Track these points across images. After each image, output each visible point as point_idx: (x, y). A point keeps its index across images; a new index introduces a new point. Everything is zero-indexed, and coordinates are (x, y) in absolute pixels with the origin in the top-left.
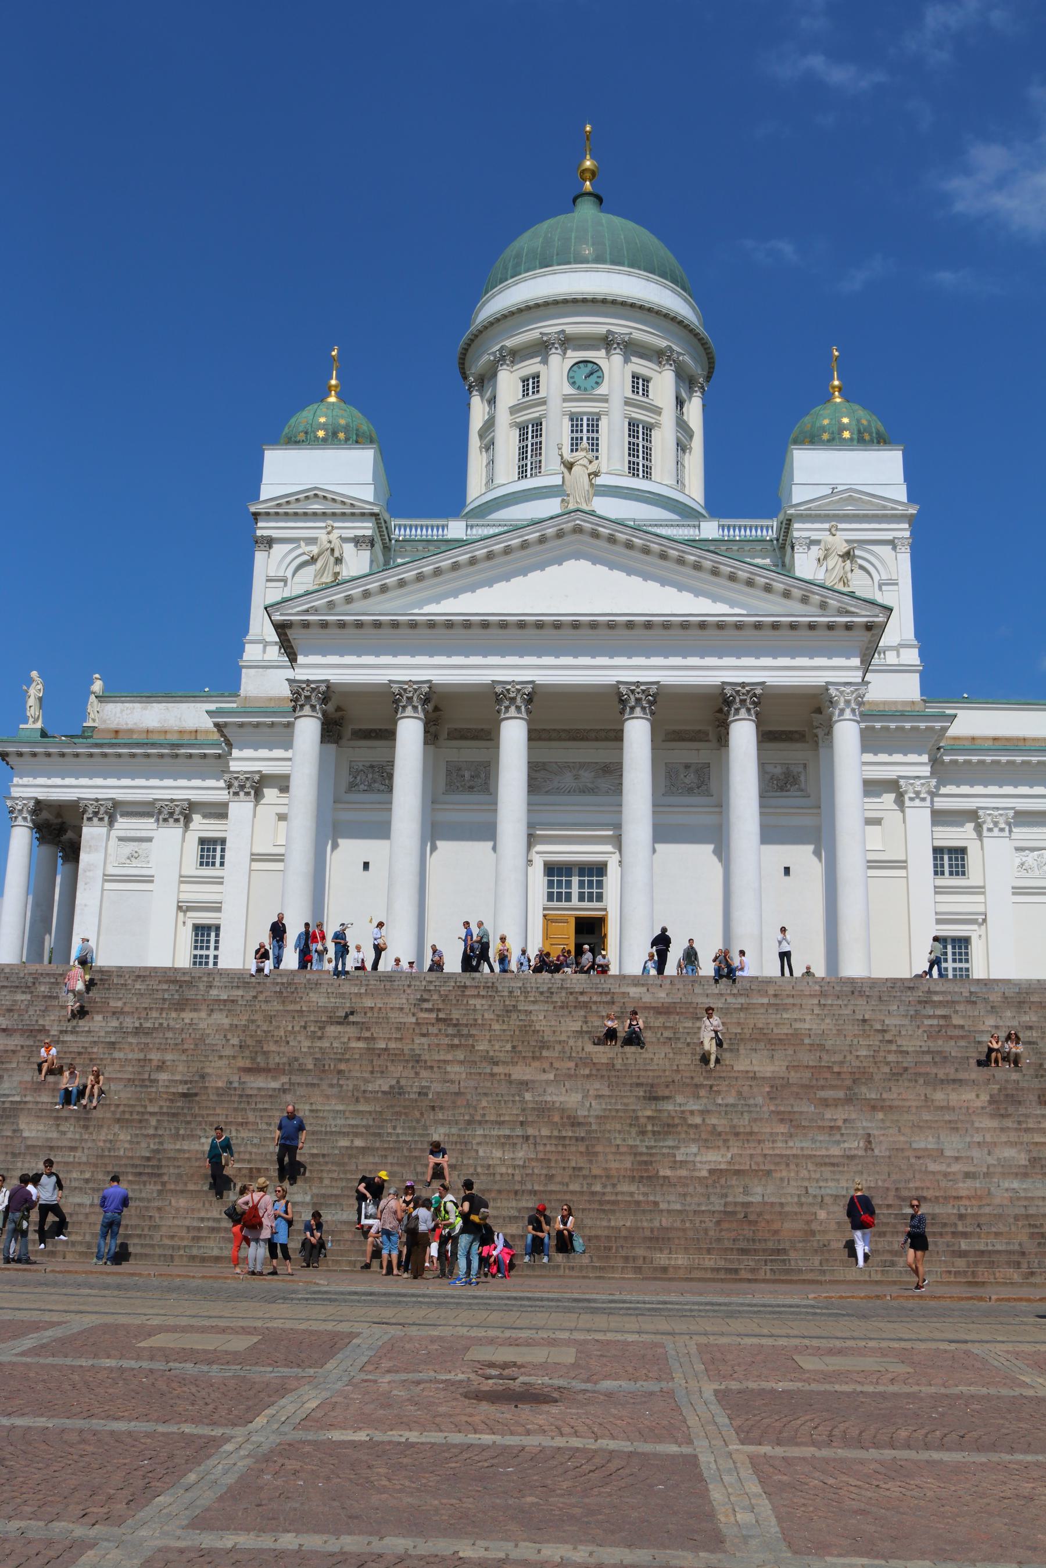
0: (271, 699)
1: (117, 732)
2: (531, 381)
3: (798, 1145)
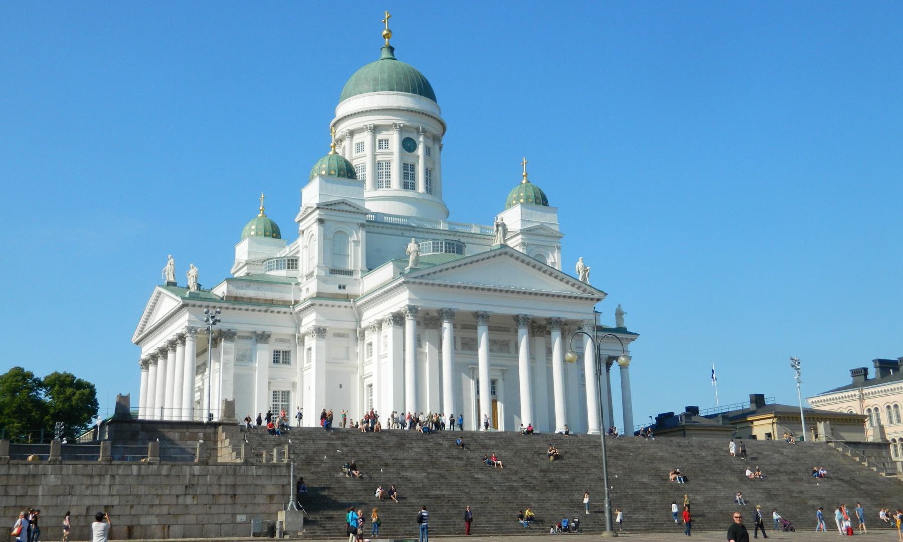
0: (330, 294)
1: (236, 298)
2: (384, 142)
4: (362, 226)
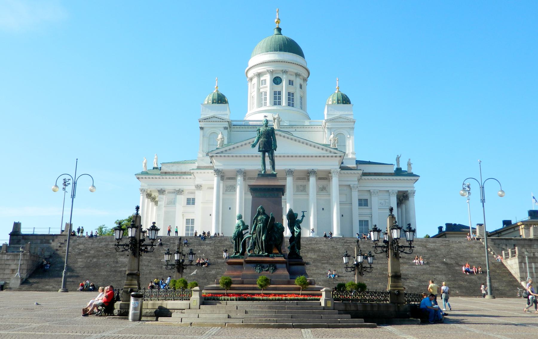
0: (204, 166)
1: (166, 172)
3: (317, 271)
4: (226, 128)
